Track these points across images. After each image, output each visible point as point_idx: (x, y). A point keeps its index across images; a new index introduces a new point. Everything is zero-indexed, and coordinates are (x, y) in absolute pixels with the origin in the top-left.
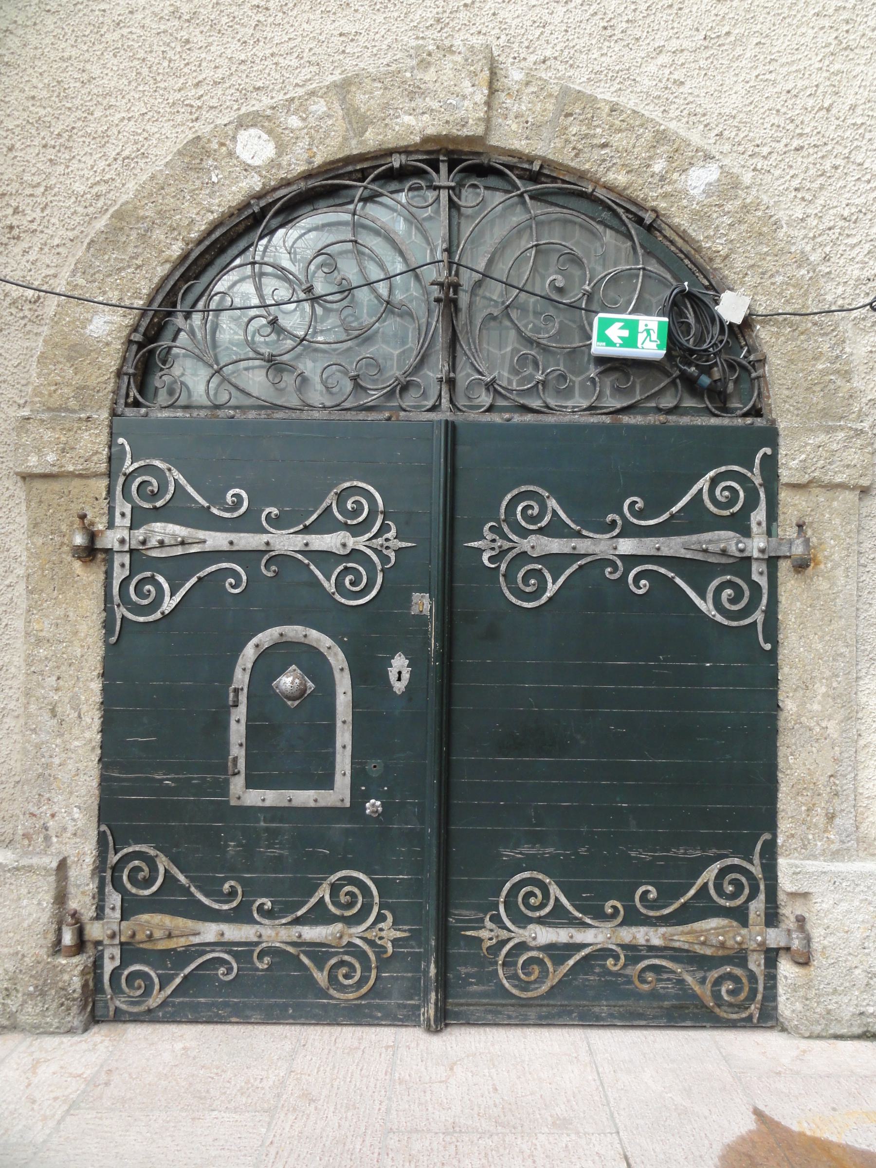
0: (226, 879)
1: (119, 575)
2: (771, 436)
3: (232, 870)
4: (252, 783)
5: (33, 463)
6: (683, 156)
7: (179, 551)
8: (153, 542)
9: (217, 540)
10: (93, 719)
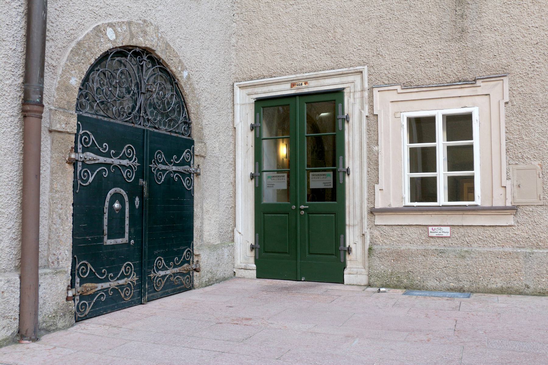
0: (102, 269)
1: (79, 169)
2: (192, 142)
3: (104, 266)
4: (108, 238)
5: (58, 127)
6: (184, 69)
7: (93, 162)
8: (88, 159)
9: (102, 159)
10: (71, 219)
